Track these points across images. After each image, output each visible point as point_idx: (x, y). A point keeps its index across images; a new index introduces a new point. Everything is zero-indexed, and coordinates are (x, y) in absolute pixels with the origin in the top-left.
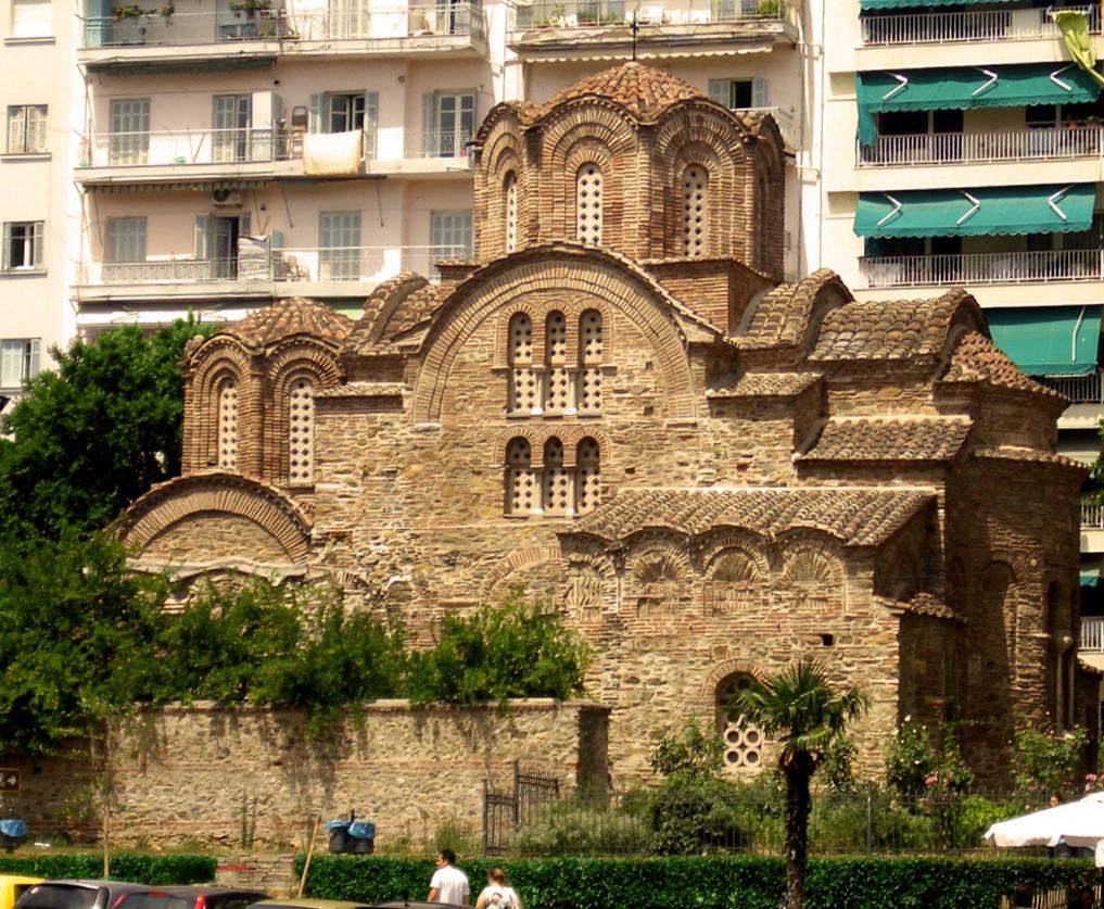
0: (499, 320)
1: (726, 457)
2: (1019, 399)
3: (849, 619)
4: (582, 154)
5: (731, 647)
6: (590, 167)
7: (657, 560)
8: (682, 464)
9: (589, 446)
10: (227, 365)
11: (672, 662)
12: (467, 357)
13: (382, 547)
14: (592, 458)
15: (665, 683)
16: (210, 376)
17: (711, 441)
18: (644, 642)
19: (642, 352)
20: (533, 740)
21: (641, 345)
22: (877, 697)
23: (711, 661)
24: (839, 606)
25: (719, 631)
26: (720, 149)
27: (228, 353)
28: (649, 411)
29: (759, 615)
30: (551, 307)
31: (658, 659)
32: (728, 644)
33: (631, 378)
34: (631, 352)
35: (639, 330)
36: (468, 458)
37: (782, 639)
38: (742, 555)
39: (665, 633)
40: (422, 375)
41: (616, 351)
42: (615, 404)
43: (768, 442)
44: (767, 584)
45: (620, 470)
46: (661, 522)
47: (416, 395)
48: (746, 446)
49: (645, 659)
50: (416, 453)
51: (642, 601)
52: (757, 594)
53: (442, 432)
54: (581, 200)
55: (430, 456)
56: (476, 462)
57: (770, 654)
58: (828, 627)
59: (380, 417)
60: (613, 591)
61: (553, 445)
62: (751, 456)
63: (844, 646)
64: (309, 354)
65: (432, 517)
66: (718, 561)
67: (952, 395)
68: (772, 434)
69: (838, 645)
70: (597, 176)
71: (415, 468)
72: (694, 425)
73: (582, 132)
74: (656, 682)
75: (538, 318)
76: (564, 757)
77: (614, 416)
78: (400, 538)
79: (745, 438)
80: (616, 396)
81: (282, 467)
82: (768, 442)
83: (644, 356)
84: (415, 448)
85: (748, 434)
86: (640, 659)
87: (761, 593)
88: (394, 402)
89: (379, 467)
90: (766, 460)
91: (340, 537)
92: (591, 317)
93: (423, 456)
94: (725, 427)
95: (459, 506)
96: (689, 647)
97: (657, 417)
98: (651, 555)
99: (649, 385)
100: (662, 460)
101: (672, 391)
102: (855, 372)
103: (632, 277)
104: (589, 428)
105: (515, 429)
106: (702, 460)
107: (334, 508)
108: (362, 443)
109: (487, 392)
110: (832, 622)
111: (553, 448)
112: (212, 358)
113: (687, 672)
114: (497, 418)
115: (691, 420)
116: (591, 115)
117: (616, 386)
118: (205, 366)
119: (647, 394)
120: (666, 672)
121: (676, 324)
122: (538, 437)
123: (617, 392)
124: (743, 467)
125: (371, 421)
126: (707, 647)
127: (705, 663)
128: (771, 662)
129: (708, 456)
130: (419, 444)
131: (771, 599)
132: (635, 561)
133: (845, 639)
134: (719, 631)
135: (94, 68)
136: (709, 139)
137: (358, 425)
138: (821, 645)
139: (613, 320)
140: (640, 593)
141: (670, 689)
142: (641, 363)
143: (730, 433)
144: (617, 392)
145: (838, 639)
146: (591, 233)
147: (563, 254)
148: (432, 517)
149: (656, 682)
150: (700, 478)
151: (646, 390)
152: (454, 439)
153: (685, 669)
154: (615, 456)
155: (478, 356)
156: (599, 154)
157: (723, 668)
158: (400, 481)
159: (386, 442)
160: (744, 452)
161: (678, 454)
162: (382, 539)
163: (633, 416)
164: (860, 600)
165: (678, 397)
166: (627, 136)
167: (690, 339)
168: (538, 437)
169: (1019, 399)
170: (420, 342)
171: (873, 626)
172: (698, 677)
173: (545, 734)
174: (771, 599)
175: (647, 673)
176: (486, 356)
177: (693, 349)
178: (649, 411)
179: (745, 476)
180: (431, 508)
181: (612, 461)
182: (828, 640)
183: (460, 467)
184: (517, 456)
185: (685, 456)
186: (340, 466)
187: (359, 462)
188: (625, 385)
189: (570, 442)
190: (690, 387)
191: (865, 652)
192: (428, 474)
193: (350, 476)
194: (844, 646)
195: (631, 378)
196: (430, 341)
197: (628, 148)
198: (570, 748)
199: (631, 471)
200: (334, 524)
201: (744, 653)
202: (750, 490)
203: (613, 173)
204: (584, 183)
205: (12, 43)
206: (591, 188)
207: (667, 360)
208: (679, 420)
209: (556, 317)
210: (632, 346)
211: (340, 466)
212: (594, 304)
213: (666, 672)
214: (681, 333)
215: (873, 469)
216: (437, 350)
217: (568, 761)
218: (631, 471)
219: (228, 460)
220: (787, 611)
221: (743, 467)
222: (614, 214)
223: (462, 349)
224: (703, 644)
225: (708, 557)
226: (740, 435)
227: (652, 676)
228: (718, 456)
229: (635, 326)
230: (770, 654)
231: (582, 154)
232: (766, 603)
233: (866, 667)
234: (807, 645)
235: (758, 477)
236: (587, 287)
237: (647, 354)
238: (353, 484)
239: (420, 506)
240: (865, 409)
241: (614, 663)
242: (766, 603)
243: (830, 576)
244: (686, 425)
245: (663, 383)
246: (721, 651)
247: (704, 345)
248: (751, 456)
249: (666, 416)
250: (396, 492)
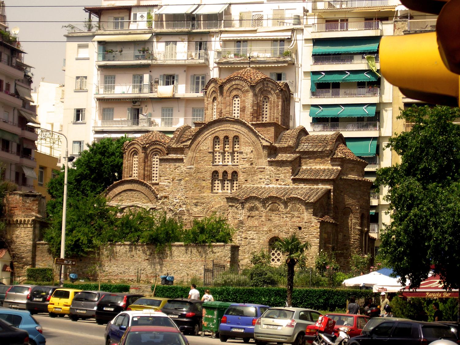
0: (211, 138)
1: (273, 177)
2: (354, 163)
3: (306, 222)
4: (235, 93)
5: (273, 230)
6: (237, 96)
7: (253, 205)
8: (261, 179)
9: (235, 173)
10: (135, 149)
11: (257, 234)
12: (202, 148)
13: (177, 200)
14: (236, 177)
16: (130, 152)
17: (269, 173)
19: (250, 148)
20: (218, 254)
21: (250, 146)
22: (313, 244)
24: (303, 219)
26: (272, 92)
27: (136, 146)
28: (252, 164)
29: (281, 221)
30: (225, 135)
31: (253, 233)
33: (247, 155)
34: (247, 148)
35: (249, 142)
36: (202, 176)
38: (277, 204)
39: (255, 225)
40: (189, 153)
43: (285, 173)
45: (243, 180)
46: (254, 195)
47: (187, 158)
48: (278, 174)
49: (249, 232)
50: (187, 174)
51: (249, 216)
53: (194, 169)
54: (234, 105)
55: (191, 175)
56: (204, 177)
58: (300, 225)
59: (177, 164)
60: (241, 213)
61: (225, 173)
64: (158, 147)
65: (191, 192)
66: (270, 206)
67: (335, 161)
68: (285, 171)
69: (303, 230)
71: (187, 178)
72: (264, 168)
73: (235, 87)
74: (252, 239)
75: (222, 138)
77: (242, 165)
78: (182, 198)
80: (242, 160)
81: (150, 178)
82: (285, 173)
84: (187, 173)
88: (181, 160)
89: (177, 178)
91: (166, 197)
92: (236, 138)
93: (189, 175)
94: (273, 169)
95: (199, 189)
97: (254, 166)
100: (255, 178)
101: (258, 159)
102: (309, 154)
103: (248, 127)
104: (235, 168)
105: (215, 168)
106: (266, 178)
107: (164, 189)
108: (172, 171)
109: (207, 158)
110: (301, 223)
111: (225, 174)
112: (131, 147)
114: (210, 165)
115: (263, 167)
116: (237, 82)
117: (243, 157)
118: (129, 149)
119: (251, 159)
120: (255, 236)
121: (260, 140)
122: (221, 170)
124: (277, 180)
125: (175, 165)
127: (266, 234)
128: (284, 234)
129: (268, 177)
130: (188, 172)
131: (284, 216)
132: (247, 205)
133: (305, 228)
135: (100, 67)
136: (270, 89)
137: (171, 166)
139: (242, 139)
140: (248, 214)
141: (256, 241)
143: (274, 171)
145: (303, 228)
146: (236, 114)
148: (191, 192)
149: (252, 239)
150: (265, 183)
152: (198, 171)
153: (260, 235)
155: (205, 148)
156: (239, 93)
157: (271, 235)
158: (182, 182)
159: (179, 171)
161: (260, 176)
162: (177, 198)
163: (247, 165)
164: (309, 217)
166: (247, 88)
167: (263, 144)
168: (221, 170)
169: (354, 163)
170: (189, 144)
171: (312, 224)
174: (284, 216)
175: (250, 236)
176: (207, 148)
177: (264, 147)
178: (252, 164)
179: (278, 182)
180: (191, 190)
181: (241, 178)
182: (300, 228)
183: (199, 178)
184: (215, 176)
185: (261, 177)
186: (166, 178)
187: (171, 177)
188: (245, 157)
189: (230, 172)
190: (263, 158)
191: (310, 232)
192: (190, 180)
193: (169, 180)
195: (247, 155)
196: (191, 144)
197: (247, 91)
199: (246, 181)
200: (164, 194)
201: (277, 231)
202: (279, 186)
204: (235, 101)
205: (77, 59)
206: (237, 102)
207: (257, 150)
208: (260, 167)
209: (226, 138)
210: (247, 146)
211: (166, 178)
212: (237, 134)
213: (255, 236)
214: (261, 143)
215: (313, 181)
216: (193, 146)
217: (227, 260)
218: (246, 181)
219: (135, 175)
221: (277, 180)
222: (243, 110)
223: (200, 146)
225: (267, 205)
227: (251, 237)
228: (270, 177)
231: (235, 93)
232: (283, 218)
233: (311, 236)
235: (281, 183)
236: (235, 130)
237: (251, 148)
238: (170, 183)
239: (188, 189)
240: (311, 165)
241: (241, 233)
242: (283, 218)
244: (262, 168)
245: (256, 156)
246: (270, 231)
247: (267, 146)
250: (181, 185)
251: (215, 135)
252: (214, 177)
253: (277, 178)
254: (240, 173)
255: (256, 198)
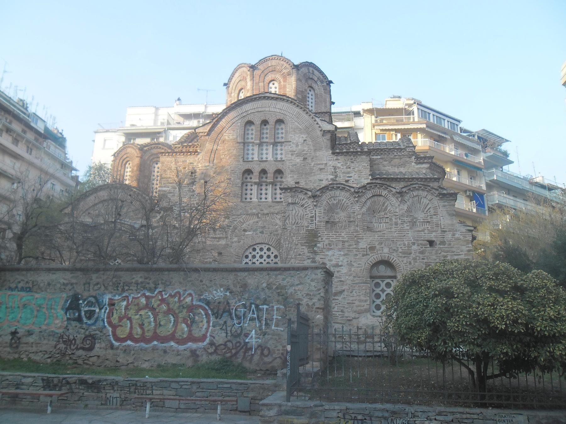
0: (240, 123)
4: (270, 77)
5: (378, 247)
7: (335, 202)
8: (320, 180)
11: (344, 255)
12: (227, 138)
14: (279, 179)
15: (341, 266)
16: (121, 160)
18: (329, 244)
19: (303, 136)
21: (301, 133)
23: (367, 255)
25: (371, 238)
26: (319, 83)
28: (305, 159)
29: (393, 230)
30: (263, 118)
32: (376, 245)
33: (297, 146)
34: (297, 136)
35: (300, 127)
37: (406, 243)
38: (381, 199)
39: (341, 239)
41: (290, 135)
42: (290, 156)
44: (397, 214)
48: (349, 173)
49: (330, 253)
51: (327, 222)
52: (391, 220)
57: (400, 250)
58: (432, 236)
60: (312, 217)
61: (264, 172)
62: (351, 177)
63: (441, 246)
67: (423, 163)
69: (438, 246)
70: (276, 84)
73: (270, 69)
76: (314, 304)
79: (349, 170)
80: (290, 153)
83: (303, 137)
85: (350, 168)
86: (327, 253)
87: (394, 219)
90: (358, 178)
92: (280, 121)
96: (355, 246)
98: (332, 199)
99: (305, 149)
100: (311, 178)
101: (315, 150)
104: (280, 166)
110: (434, 234)
113: (353, 260)
115: (325, 162)
116: (274, 63)
120: (343, 260)
122: (256, 169)
123: (290, 151)
126: (365, 247)
127: (363, 255)
128: (401, 255)
129: (332, 177)
131: (399, 222)
132: (325, 198)
133: (443, 243)
134: (371, 238)
136: (316, 79)
138: (428, 246)
140: (326, 219)
142: (301, 140)
143: (342, 167)
144: (290, 151)
147: (269, 97)
151: (304, 151)
154: (291, 177)
156: (278, 76)
157: (374, 258)
160: (348, 175)
161: (318, 176)
165: (318, 153)
166: (289, 69)
167: (323, 129)
170: (207, 131)
171: (457, 236)
172: (360, 263)
173: (299, 286)
174: (399, 222)
175: (330, 260)
181: (289, 179)
182: (431, 243)
184: (246, 178)
189: (271, 170)
194: (441, 246)
195: (297, 146)
196: (211, 130)
197: (289, 74)
198: (318, 296)
201: (386, 250)
203: (282, 83)
209: (265, 122)
213: (343, 260)
214: (320, 127)
216: (213, 134)
217: (317, 305)
220: (408, 228)
223: (225, 134)
224: (363, 245)
225: (363, 200)
226: (346, 168)
227: (334, 262)
229: (299, 126)
230: (400, 250)
232: (396, 224)
234: (421, 246)
236: (278, 111)
237: (304, 136)
242: (396, 224)
243: (431, 209)
244: (322, 164)
245: (312, 148)
247: (329, 131)
248: (351, 177)
249: (312, 161)
251: (246, 119)
252: (244, 180)
253: (347, 179)
254: (287, 173)
255: (342, 187)
